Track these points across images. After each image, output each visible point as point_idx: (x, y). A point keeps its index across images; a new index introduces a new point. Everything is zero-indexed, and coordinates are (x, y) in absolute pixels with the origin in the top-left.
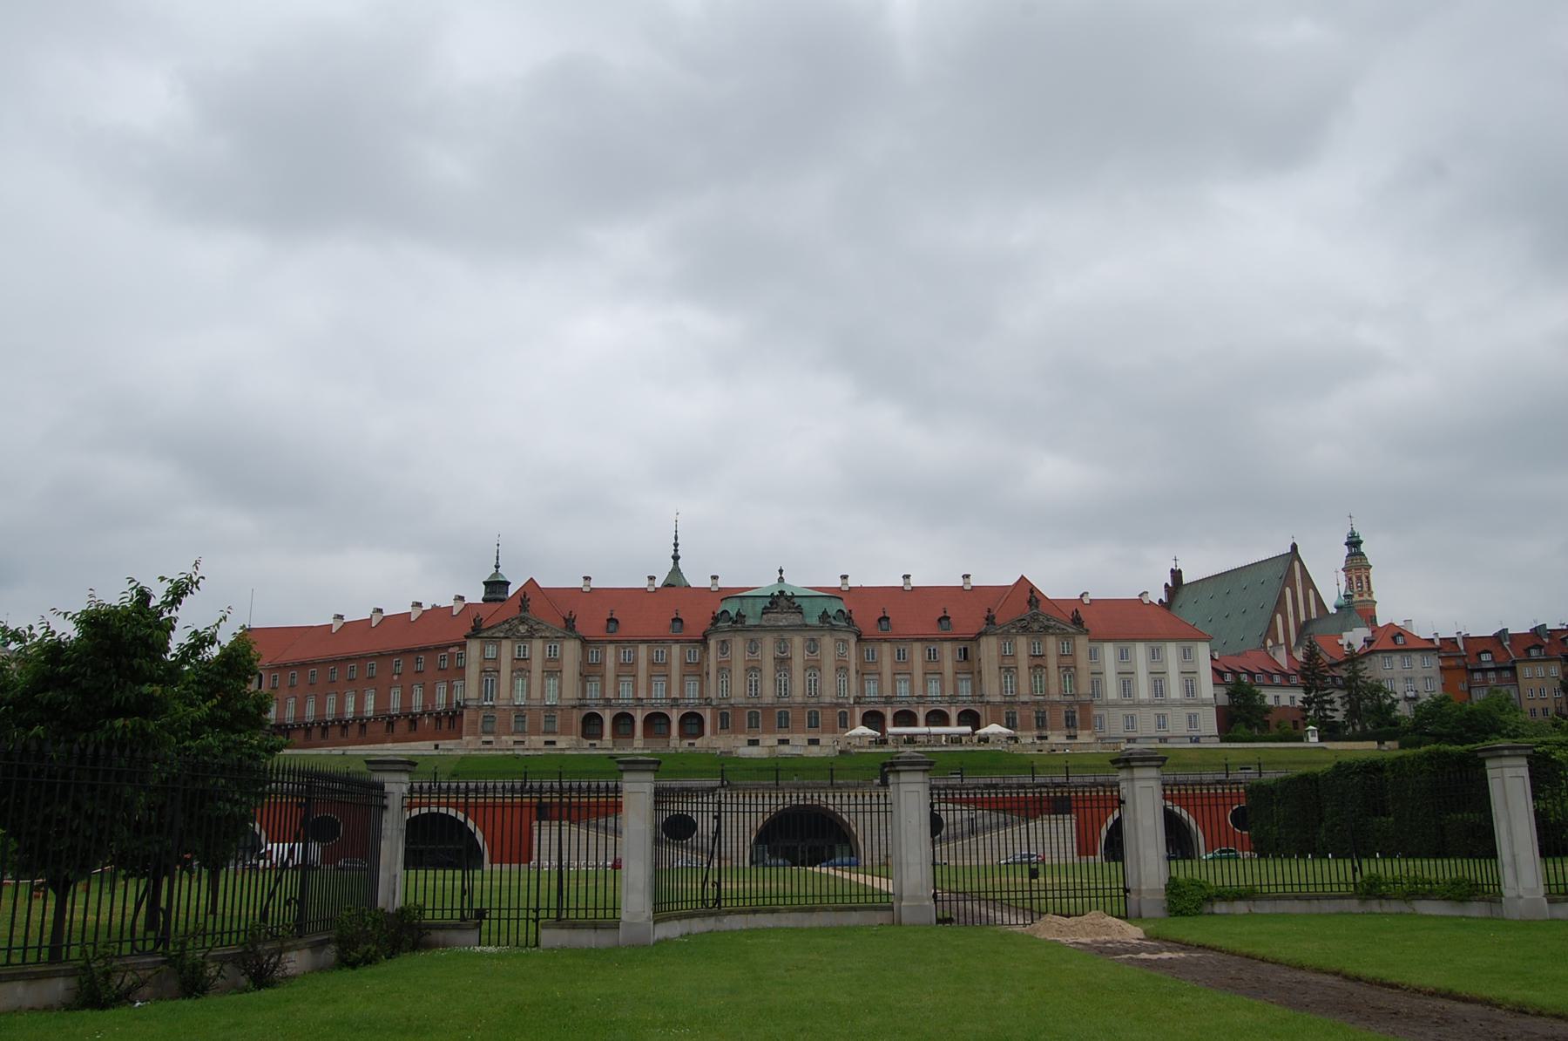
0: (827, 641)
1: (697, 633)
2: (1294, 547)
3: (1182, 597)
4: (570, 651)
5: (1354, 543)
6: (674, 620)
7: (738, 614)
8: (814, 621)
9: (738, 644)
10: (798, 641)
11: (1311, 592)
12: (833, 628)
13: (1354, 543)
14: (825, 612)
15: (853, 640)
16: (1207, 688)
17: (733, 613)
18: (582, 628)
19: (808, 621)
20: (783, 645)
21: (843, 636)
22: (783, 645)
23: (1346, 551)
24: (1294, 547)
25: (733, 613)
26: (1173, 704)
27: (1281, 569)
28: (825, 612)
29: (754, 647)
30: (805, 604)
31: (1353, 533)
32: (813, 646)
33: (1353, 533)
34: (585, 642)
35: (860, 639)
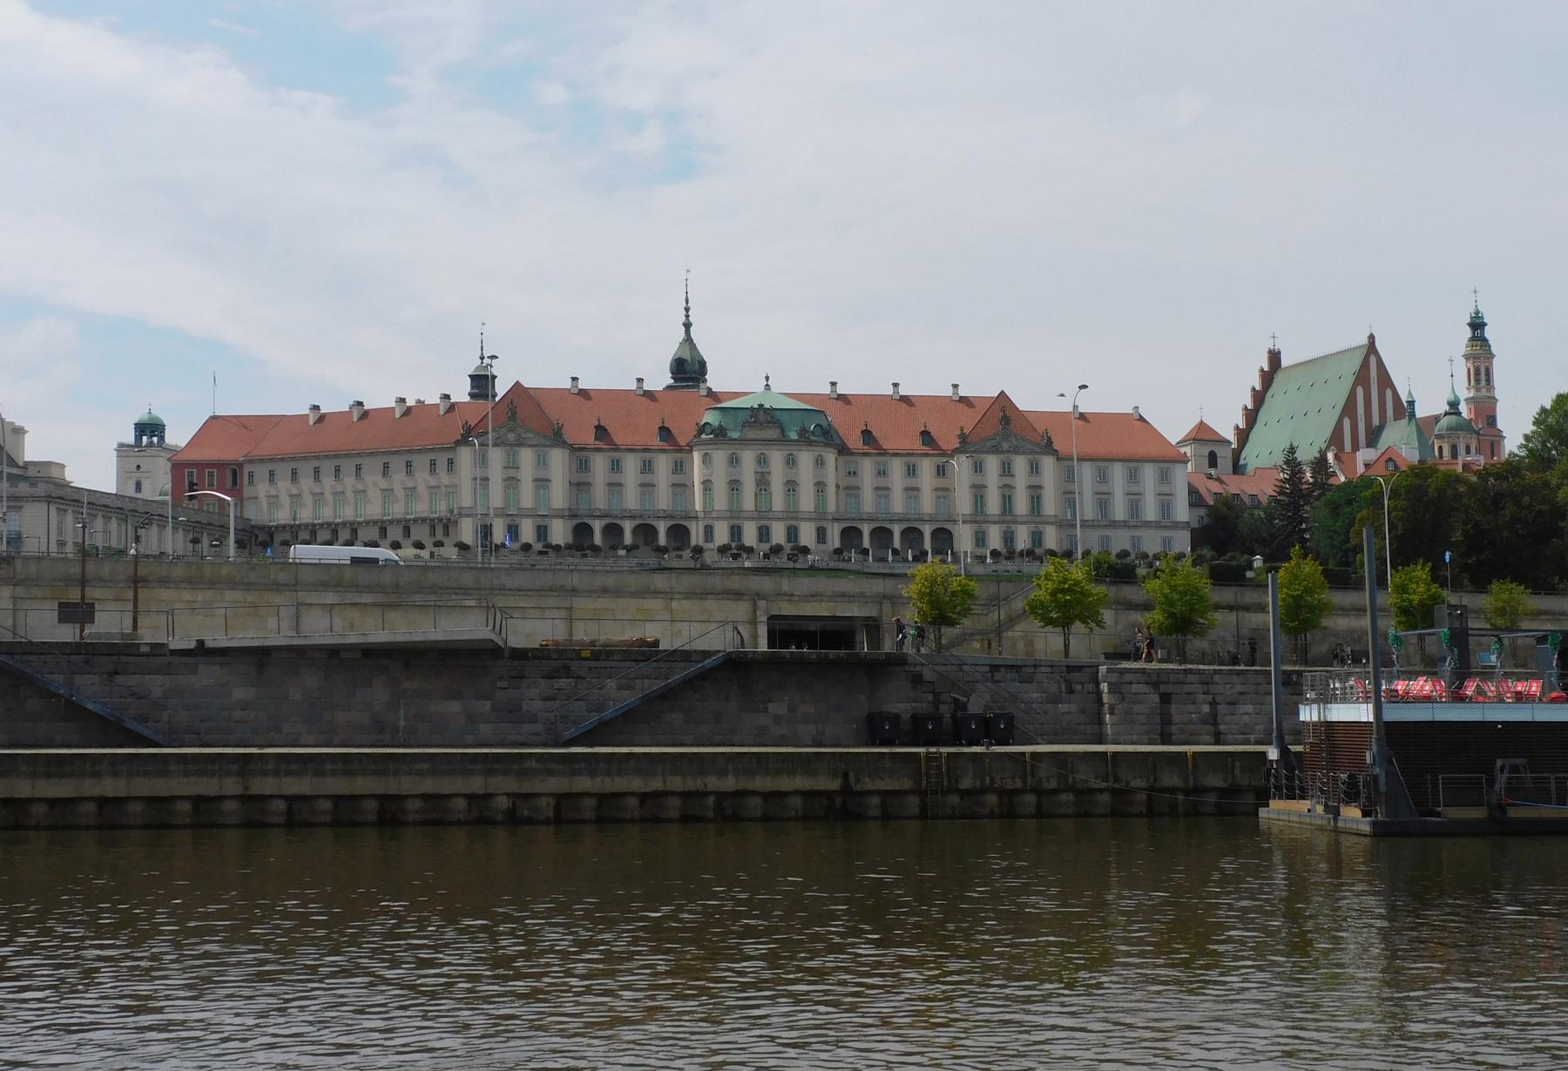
0: (806, 458)
2: (1372, 338)
3: (1279, 379)
4: (558, 460)
5: (1477, 325)
8: (794, 436)
9: (720, 456)
10: (776, 458)
11: (1389, 393)
13: (1477, 325)
16: (1182, 512)
18: (568, 437)
20: (762, 461)
22: (762, 461)
23: (1468, 333)
24: (1372, 338)
26: (1148, 525)
27: (1355, 364)
31: (1477, 312)
32: (791, 462)
33: (1477, 312)
34: (574, 449)
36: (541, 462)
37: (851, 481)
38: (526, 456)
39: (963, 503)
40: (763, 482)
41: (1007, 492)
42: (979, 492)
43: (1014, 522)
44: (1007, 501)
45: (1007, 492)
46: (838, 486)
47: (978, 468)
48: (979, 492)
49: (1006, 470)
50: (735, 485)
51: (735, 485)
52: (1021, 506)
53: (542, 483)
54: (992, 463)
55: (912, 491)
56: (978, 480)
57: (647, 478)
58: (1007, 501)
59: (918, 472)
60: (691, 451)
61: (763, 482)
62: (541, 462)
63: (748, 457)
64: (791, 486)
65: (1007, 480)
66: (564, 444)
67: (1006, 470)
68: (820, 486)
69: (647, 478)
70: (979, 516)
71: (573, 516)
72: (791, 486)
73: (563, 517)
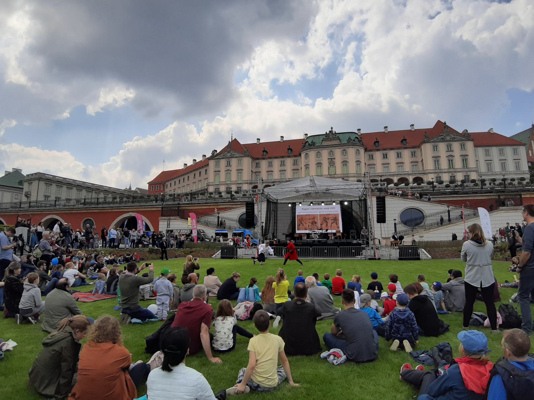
0: (351, 151)
1: (297, 154)
6: (288, 149)
7: (312, 142)
8: (345, 142)
9: (312, 154)
10: (338, 152)
12: (354, 145)
14: (350, 138)
15: (362, 151)
17: (310, 142)
19: (343, 142)
21: (358, 148)
25: (310, 142)
28: (350, 138)
29: (318, 155)
30: (340, 136)
34: (254, 159)
35: (366, 150)
36: (240, 163)
37: (371, 162)
38: (234, 162)
39: (430, 165)
40: (332, 162)
41: (451, 158)
42: (436, 159)
43: (455, 172)
44: (451, 162)
45: (451, 158)
46: (365, 164)
47: (435, 148)
48: (436, 159)
49: (449, 149)
50: (319, 165)
51: (319, 165)
52: (458, 164)
53: (240, 171)
54: (442, 146)
55: (400, 164)
56: (436, 154)
57: (283, 168)
58: (451, 162)
59: (403, 156)
60: (300, 155)
61: (332, 162)
62: (240, 163)
63: (325, 153)
64: (345, 163)
65: (450, 153)
66: (248, 156)
67: (449, 149)
68: (358, 162)
69: (283, 168)
70: (438, 170)
71: (251, 183)
72: (345, 163)
73: (247, 183)
